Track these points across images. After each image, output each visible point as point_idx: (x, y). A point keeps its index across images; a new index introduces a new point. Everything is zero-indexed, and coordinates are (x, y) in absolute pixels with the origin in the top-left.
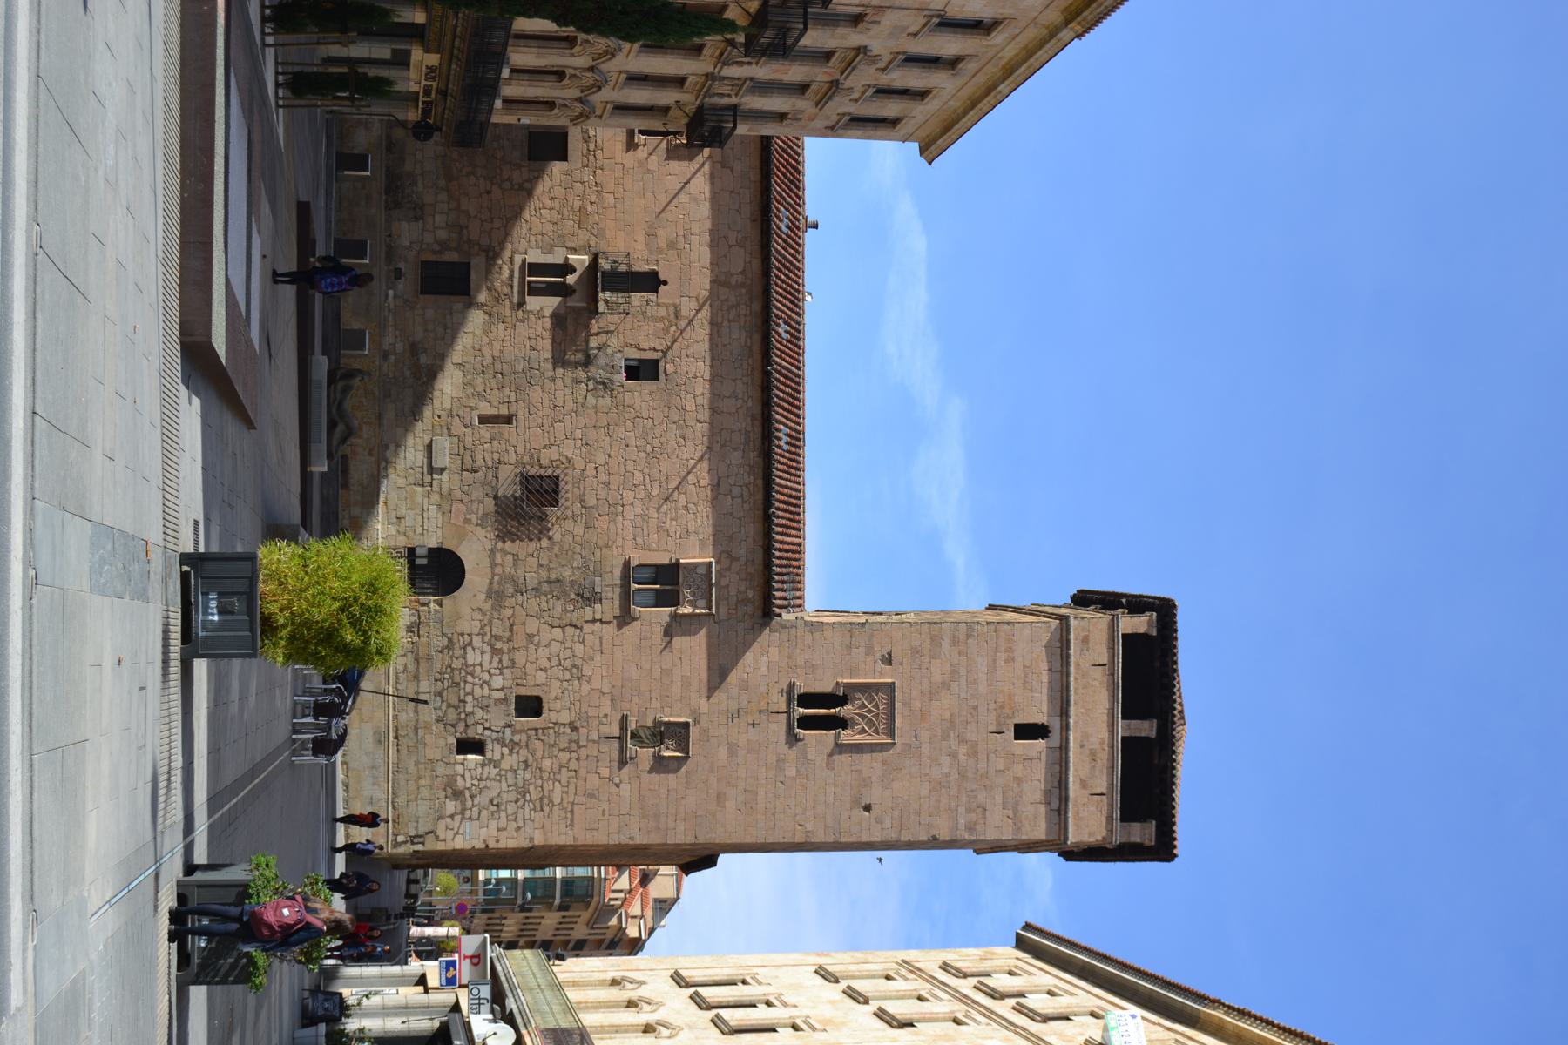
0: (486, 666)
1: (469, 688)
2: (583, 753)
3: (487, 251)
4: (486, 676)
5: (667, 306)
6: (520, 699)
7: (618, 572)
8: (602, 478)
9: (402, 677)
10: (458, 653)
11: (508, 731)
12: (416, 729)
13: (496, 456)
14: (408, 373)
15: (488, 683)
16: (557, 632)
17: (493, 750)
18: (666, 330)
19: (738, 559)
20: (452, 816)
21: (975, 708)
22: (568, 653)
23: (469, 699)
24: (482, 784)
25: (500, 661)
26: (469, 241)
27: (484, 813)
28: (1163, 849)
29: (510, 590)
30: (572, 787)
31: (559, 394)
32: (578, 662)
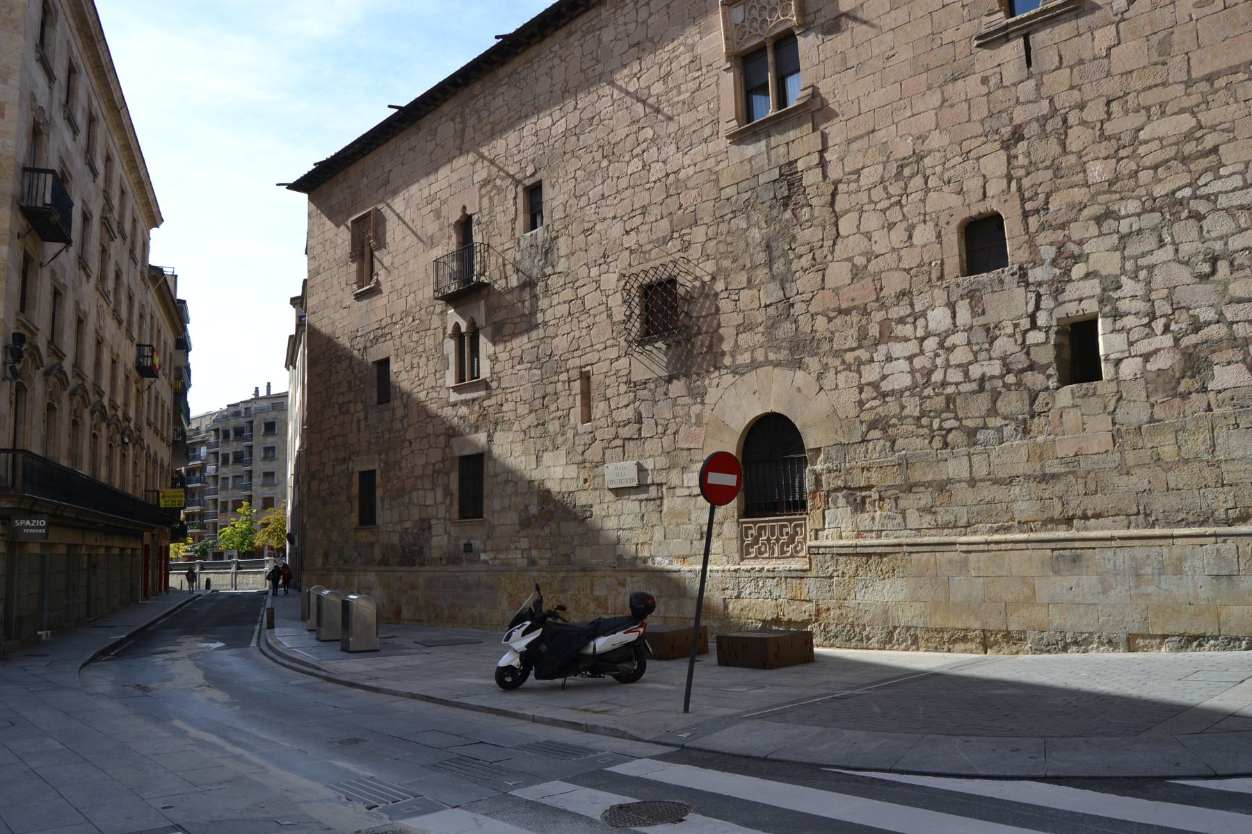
0: (912, 347)
1: (955, 376)
2: (1065, 100)
4: (931, 344)
6: (972, 266)
11: (1036, 274)
12: (1045, 478)
13: (623, 388)
16: (846, 225)
17: (1082, 297)
22: (878, 193)
23: (975, 371)
24: (1163, 308)
25: (902, 321)
29: (786, 328)
30: (1150, 98)
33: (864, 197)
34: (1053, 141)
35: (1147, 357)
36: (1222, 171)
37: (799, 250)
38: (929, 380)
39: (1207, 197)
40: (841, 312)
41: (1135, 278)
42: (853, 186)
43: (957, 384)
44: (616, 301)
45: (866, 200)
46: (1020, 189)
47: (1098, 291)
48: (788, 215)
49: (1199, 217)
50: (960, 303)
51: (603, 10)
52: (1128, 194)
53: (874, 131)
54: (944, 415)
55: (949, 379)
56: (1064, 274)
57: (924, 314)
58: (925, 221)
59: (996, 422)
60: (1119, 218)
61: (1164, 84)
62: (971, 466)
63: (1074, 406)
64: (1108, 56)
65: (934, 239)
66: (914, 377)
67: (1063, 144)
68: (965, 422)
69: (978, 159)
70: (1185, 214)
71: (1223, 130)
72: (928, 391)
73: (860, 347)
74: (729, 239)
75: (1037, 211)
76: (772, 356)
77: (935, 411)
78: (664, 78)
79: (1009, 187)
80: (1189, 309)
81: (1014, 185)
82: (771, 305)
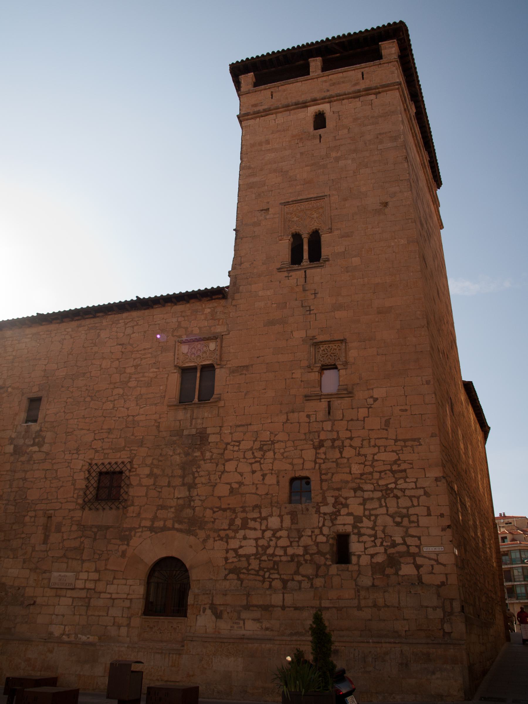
0: (259, 534)
2: (344, 434)
4: (268, 534)
9: (266, 624)
13: (74, 528)
15: (275, 531)
17: (344, 523)
19: (179, 323)
20: (418, 567)
21: (302, 154)
22: (249, 455)
23: (290, 551)
25: (254, 519)
27: (412, 531)
28: (398, 32)
29: (188, 512)
30: (380, 443)
32: (257, 445)
33: (241, 455)
34: (337, 450)
35: (372, 556)
36: (407, 480)
37: (202, 473)
38: (266, 551)
39: (401, 490)
40: (220, 509)
41: (369, 519)
42: (236, 448)
43: (280, 556)
45: (242, 456)
46: (319, 468)
47: (352, 522)
48: (198, 454)
49: (397, 497)
50: (286, 516)
51: (104, 321)
52: (368, 481)
53: (250, 424)
54: (272, 571)
55: (276, 553)
56: (337, 511)
57: (266, 518)
58: (272, 474)
59: (298, 578)
60: (363, 491)
61: (387, 439)
62: (284, 599)
63: (337, 575)
64: (364, 421)
65: (275, 483)
67: (341, 453)
68: (282, 576)
69: (302, 450)
70: (392, 495)
71: (408, 463)
72: (264, 558)
73: (229, 529)
74: (161, 458)
75: (326, 480)
76: (177, 526)
77: (267, 568)
78: (136, 367)
79: (315, 467)
80: (391, 537)
81: (317, 466)
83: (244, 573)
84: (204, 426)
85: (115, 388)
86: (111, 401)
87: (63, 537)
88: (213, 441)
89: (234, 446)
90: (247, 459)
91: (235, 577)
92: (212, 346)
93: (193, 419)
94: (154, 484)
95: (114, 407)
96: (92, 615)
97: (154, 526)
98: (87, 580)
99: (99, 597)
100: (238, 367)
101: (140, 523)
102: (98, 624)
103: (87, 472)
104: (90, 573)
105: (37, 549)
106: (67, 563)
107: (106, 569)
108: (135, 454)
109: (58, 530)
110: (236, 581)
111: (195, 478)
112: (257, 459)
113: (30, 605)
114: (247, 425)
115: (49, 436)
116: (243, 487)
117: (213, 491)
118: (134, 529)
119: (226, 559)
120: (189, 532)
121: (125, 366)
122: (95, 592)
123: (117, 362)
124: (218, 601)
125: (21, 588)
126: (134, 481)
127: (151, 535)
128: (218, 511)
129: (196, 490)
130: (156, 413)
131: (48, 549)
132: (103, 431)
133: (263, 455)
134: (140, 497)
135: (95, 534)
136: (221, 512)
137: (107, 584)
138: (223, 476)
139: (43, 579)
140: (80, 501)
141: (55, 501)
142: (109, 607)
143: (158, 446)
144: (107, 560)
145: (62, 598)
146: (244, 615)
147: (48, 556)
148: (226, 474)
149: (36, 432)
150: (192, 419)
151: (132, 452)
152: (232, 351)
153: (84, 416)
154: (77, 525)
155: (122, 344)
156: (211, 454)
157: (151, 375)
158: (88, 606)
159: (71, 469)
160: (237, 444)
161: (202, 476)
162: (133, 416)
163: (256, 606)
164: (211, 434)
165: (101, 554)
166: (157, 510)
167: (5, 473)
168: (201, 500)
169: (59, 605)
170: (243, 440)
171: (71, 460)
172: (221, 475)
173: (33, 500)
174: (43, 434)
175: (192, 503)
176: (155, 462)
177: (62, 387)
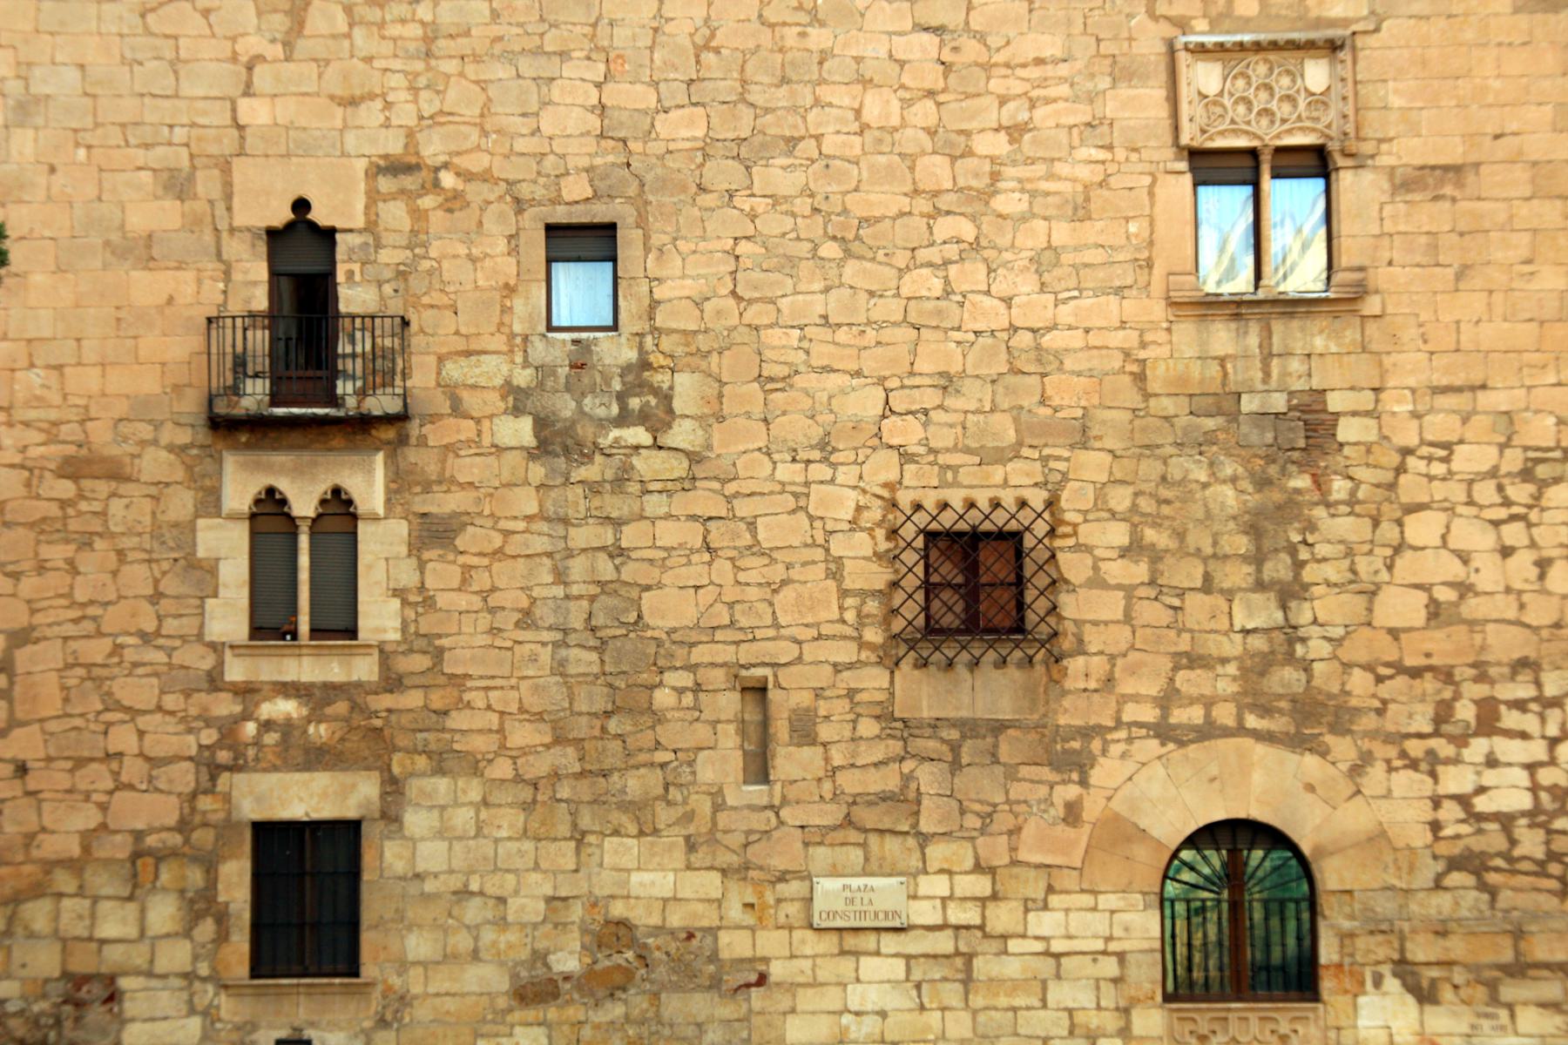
0: (1538, 750)
3: (215, 770)
5: (373, 197)
7: (1222, 337)
8: (930, 398)
10: (1494, 839)
13: (868, 728)
14: (616, 1010)
18: (453, 202)
22: (1486, 492)
25: (1520, 705)
26: (183, 826)
29: (1287, 678)
31: (669, 534)
32: (1513, 460)
33: (1457, 492)
37: (1322, 550)
40: (1400, 669)
42: (1438, 469)
44: (860, 553)
45: (1463, 498)
48: (1302, 482)
53: (1484, 387)
66: (1536, 798)
73: (1436, 733)
76: (1252, 721)
78: (1015, 132)
82: (1255, 630)
83: (1497, 870)
84: (1316, 383)
85: (938, 212)
86: (930, 265)
87: (827, 760)
88: (1353, 439)
89: (1430, 459)
90: (1481, 507)
91: (1470, 880)
92: (1316, 74)
93: (1271, 355)
94: (1152, 583)
95: (948, 293)
96: (987, 1008)
97: (1172, 720)
98: (951, 897)
99: (1006, 952)
100: (1422, 168)
101: (1119, 711)
102: (1016, 1034)
103: (880, 534)
104: (957, 878)
105: (730, 801)
106: (864, 845)
107: (1015, 863)
108: (1064, 474)
109: (804, 732)
110: (1474, 893)
111: (1299, 565)
112: (1515, 510)
113: (748, 986)
114: (1473, 389)
115: (687, 390)
116: (1472, 601)
117: (1370, 610)
118: (1100, 730)
119: (1435, 826)
120: (1298, 742)
121: (964, 126)
122: (986, 936)
123: (929, 104)
124: (1420, 950)
125: (699, 935)
126: (1073, 566)
127: (1164, 750)
128: (1391, 677)
129: (1307, 605)
130: (1123, 325)
131: (777, 802)
132: (917, 381)
133: (1537, 497)
134: (1106, 623)
135: (955, 748)
136: (1401, 681)
137: (1027, 910)
138: (1399, 562)
139: (779, 901)
140: (873, 635)
141: (771, 633)
142: (1044, 983)
143: (1147, 447)
144: (1015, 832)
145: (863, 960)
146: (1508, 991)
147: (781, 823)
148: (1408, 554)
149: (626, 370)
150: (1267, 357)
151: (1052, 464)
152: (1396, 102)
153: (825, 317)
154: (878, 717)
155: (938, 30)
156: (1349, 484)
157: (1084, 173)
158: (967, 981)
159: (811, 518)
160: (1442, 453)
161: (1325, 560)
162: (1033, 331)
163: (1547, 966)
164: (1345, 414)
165: (990, 815)
166: (1176, 668)
167: (521, 525)
168: (1329, 640)
169: (858, 980)
170: (1461, 442)
171: (807, 484)
172: (1392, 558)
173: (674, 630)
174: (661, 379)
175: (1299, 650)
176: (1146, 505)
177: (701, 188)
